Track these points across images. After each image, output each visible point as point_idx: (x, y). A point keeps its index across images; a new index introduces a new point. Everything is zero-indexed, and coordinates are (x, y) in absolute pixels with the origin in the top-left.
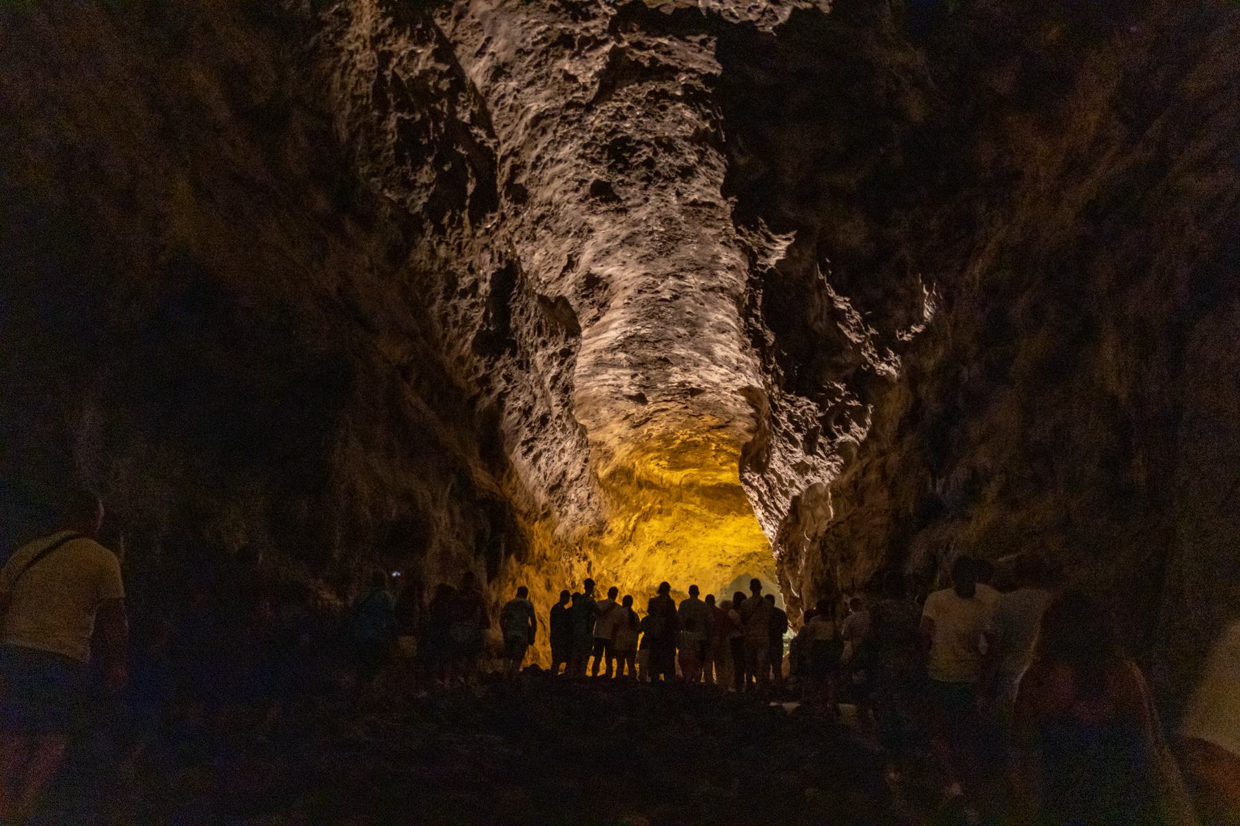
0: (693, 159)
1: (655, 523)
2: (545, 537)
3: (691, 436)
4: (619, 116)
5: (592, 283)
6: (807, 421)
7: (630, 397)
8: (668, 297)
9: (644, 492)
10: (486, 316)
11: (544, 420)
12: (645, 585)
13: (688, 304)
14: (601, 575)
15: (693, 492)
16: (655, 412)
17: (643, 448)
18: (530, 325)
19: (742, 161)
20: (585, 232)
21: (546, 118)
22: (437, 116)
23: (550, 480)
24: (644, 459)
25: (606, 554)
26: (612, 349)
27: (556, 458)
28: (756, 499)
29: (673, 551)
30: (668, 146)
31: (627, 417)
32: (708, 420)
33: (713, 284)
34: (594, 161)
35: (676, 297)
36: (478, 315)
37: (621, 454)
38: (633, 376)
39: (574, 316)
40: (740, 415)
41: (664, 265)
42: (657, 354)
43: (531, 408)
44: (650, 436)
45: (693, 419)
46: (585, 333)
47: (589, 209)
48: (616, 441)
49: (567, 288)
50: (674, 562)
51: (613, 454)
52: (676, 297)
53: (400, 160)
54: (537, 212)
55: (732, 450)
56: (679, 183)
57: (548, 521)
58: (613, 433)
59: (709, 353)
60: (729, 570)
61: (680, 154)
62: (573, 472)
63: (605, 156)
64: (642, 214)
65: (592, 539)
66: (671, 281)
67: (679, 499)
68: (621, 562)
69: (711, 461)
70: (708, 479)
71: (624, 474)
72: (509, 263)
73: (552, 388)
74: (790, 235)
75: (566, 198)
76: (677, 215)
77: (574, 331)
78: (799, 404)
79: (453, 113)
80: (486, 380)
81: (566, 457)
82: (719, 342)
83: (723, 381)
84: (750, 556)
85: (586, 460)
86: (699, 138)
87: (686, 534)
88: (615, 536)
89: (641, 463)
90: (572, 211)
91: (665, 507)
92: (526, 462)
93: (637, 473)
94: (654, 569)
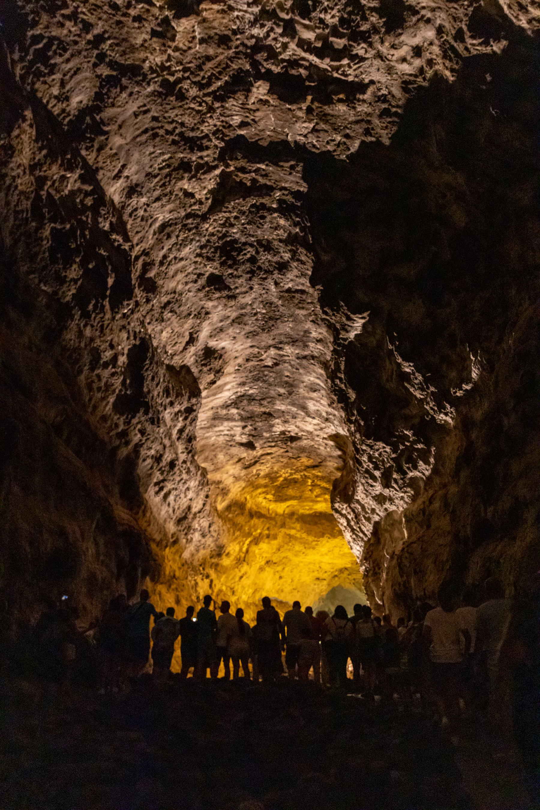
0: (287, 256)
1: (264, 546)
2: (174, 560)
3: (291, 474)
4: (228, 224)
5: (209, 354)
6: (383, 461)
7: (242, 444)
8: (270, 364)
9: (255, 521)
10: (123, 383)
11: (172, 465)
13: (286, 370)
14: (220, 591)
15: (294, 520)
16: (262, 455)
17: (253, 485)
18: (160, 389)
19: (325, 258)
20: (202, 314)
21: (170, 226)
22: (83, 225)
23: (178, 514)
24: (254, 494)
25: (224, 573)
26: (226, 406)
27: (182, 495)
28: (345, 524)
29: (279, 568)
30: (267, 246)
31: (240, 460)
32: (305, 461)
33: (306, 353)
34: (209, 259)
35: (276, 364)
36: (117, 382)
37: (236, 490)
38: (244, 427)
39: (195, 381)
40: (331, 456)
41: (266, 339)
42: (263, 409)
43: (161, 456)
44: (258, 475)
45: (293, 460)
46: (204, 394)
47: (205, 296)
48: (231, 480)
49: (189, 358)
50: (281, 578)
51: (229, 490)
52: (276, 364)
53: (53, 260)
54: (164, 299)
55: (324, 485)
56: (276, 275)
57: (176, 547)
58: (228, 474)
59: (304, 408)
60: (325, 583)
61: (276, 253)
62: (196, 507)
63: (218, 255)
64: (248, 299)
65: (213, 560)
66: (273, 352)
67: (283, 525)
68: (237, 579)
69: (308, 494)
70: (306, 508)
71: (237, 506)
72: (142, 340)
73: (178, 439)
74: (365, 315)
75: (187, 287)
76: (276, 300)
77: (196, 393)
78: (376, 447)
79: (96, 222)
80: (124, 434)
81: (190, 494)
82: (312, 399)
83: (316, 430)
84: (341, 571)
85: (207, 496)
86: (291, 240)
87: (290, 555)
88: (232, 558)
89: (251, 497)
90: (192, 298)
91: (272, 532)
92: (158, 499)
93: (249, 505)
94: (264, 584)
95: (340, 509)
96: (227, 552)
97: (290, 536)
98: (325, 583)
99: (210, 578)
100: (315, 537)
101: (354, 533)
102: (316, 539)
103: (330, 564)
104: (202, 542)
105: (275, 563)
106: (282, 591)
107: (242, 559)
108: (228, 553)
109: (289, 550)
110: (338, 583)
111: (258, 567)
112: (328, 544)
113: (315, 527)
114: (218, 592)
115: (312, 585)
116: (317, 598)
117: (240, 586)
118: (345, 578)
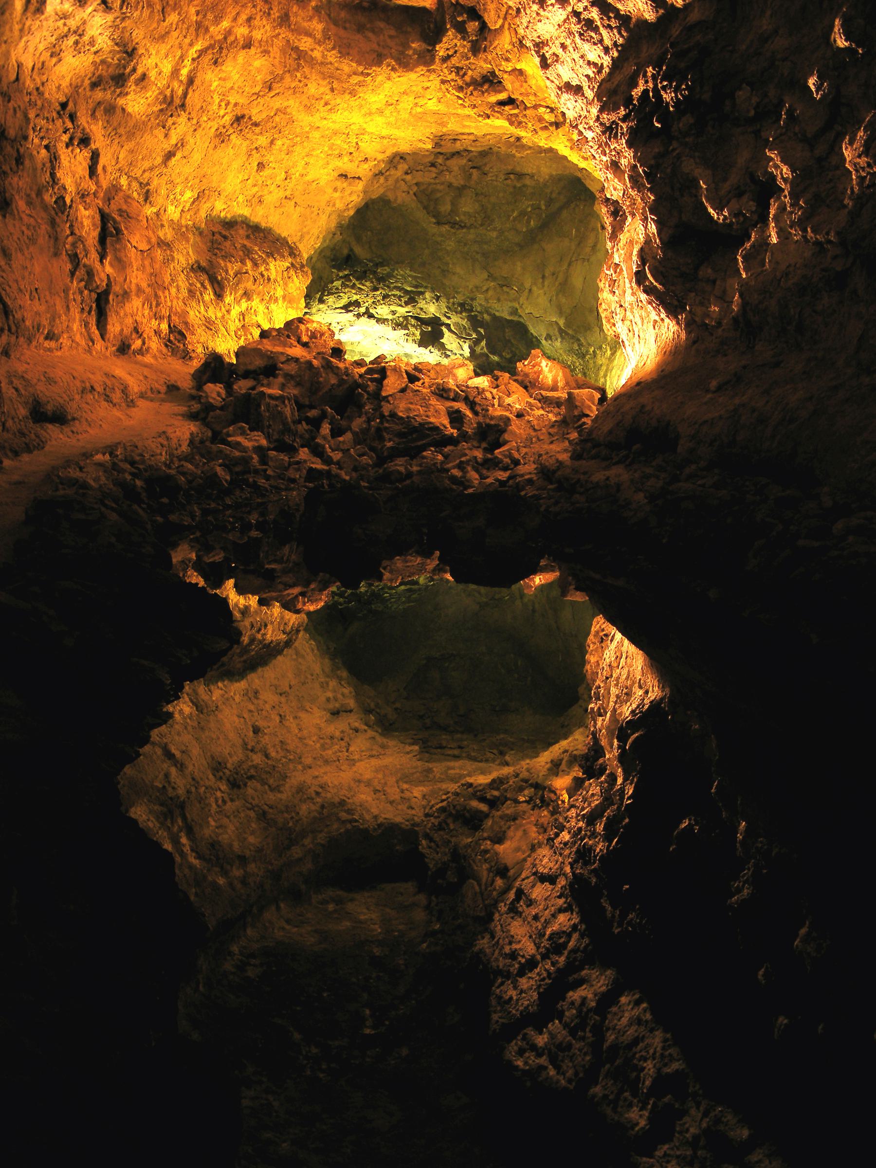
12: (203, 214)
14: (115, 188)
29: (263, 141)
50: (261, 166)
65: (99, 95)
68: (159, 160)
84: (397, 159)
87: (293, 104)
88: (151, 94)
94: (223, 180)
96: (140, 71)
97: (301, 55)
98: (360, 186)
99: (93, 146)
100: (359, 63)
102: (361, 69)
105: (256, 125)
107: (177, 101)
108: (144, 77)
110: (382, 191)
111: (213, 130)
112: (388, 84)
113: (358, 36)
114: (108, 191)
115: (330, 191)
116: (333, 225)
117: (165, 178)
118: (397, 181)
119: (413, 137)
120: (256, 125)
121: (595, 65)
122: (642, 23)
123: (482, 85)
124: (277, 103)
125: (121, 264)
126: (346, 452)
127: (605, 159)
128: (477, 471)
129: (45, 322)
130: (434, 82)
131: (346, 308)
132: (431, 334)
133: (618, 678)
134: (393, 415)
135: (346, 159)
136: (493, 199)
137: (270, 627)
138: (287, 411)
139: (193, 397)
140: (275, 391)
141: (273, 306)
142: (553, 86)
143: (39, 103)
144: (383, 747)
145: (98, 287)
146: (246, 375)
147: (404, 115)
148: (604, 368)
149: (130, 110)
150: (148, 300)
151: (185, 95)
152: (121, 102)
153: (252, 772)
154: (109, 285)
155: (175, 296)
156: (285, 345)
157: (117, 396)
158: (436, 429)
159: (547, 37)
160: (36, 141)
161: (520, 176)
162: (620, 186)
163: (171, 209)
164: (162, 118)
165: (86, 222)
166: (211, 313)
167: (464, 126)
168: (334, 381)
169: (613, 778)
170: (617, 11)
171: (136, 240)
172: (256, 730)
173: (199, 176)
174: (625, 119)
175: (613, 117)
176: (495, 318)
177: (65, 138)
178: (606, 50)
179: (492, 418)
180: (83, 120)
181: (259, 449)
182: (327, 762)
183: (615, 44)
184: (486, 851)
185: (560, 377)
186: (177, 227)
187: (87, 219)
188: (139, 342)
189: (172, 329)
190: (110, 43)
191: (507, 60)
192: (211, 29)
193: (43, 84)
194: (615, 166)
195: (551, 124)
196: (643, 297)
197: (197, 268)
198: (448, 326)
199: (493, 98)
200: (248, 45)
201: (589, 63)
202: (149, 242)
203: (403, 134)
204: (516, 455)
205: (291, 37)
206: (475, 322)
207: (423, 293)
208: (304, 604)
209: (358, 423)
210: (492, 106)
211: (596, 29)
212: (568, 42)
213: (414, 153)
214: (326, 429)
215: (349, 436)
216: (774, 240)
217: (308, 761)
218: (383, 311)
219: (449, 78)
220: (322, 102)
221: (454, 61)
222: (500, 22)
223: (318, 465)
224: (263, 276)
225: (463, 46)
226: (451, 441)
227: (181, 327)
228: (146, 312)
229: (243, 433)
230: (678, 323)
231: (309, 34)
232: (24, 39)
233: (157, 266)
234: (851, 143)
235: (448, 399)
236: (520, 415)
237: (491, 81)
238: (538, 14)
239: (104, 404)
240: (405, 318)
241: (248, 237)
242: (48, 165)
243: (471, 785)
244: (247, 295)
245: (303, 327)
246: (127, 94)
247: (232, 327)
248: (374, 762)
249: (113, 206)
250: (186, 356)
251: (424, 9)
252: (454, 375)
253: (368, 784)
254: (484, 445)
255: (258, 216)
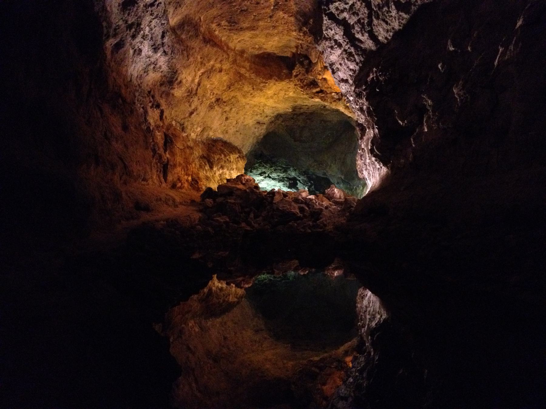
14: (171, 125)
28: (339, 37)
29: (227, 109)
50: (227, 119)
65: (163, 89)
68: (187, 115)
84: (279, 116)
87: (238, 94)
88: (183, 89)
93: (202, 29)
95: (336, 13)
96: (179, 79)
98: (265, 127)
100: (263, 78)
101: (353, 45)
102: (264, 81)
103: (273, 107)
104: (152, 60)
105: (225, 102)
106: (227, 132)
107: (194, 92)
109: (239, 89)
112: (274, 87)
115: (253, 128)
118: (279, 125)
119: (284, 107)
120: (225, 102)
121: (353, 70)
122: (371, 51)
123: (310, 86)
124: (232, 94)
125: (173, 154)
126: (259, 224)
127: (357, 107)
128: (309, 229)
129: (142, 174)
130: (292, 85)
131: (261, 174)
132: (293, 184)
133: (369, 311)
134: (278, 209)
135: (259, 116)
136: (316, 131)
137: (231, 296)
138: (237, 208)
139: (200, 204)
140: (233, 201)
141: (232, 172)
142: (337, 81)
143: (140, 90)
144: (276, 345)
145: (163, 162)
146: (221, 195)
147: (281, 98)
148: (360, 194)
149: (175, 95)
150: (183, 168)
151: (197, 89)
152: (172, 91)
153: (223, 356)
154: (168, 161)
155: (194, 166)
156: (236, 184)
157: (171, 202)
158: (294, 214)
159: (334, 61)
160: (139, 105)
161: (325, 122)
162: (363, 117)
163: (192, 134)
164: (188, 98)
165: (159, 137)
166: (208, 174)
167: (304, 102)
168: (255, 197)
169: (369, 353)
170: (361, 48)
171: (179, 145)
172: (225, 338)
173: (205, 123)
174: (364, 90)
175: (360, 90)
176: (317, 177)
177: (150, 104)
178: (357, 64)
179: (316, 209)
180: (157, 98)
181: (226, 223)
182: (253, 352)
183: (361, 61)
184: (319, 389)
185: (342, 195)
186: (195, 141)
187: (159, 136)
188: (180, 184)
189: (193, 179)
190: (167, 68)
191: (320, 74)
192: (207, 64)
193: (141, 83)
194: (361, 110)
195: (337, 99)
196: (373, 159)
197: (202, 157)
198: (299, 181)
199: (315, 91)
200: (221, 71)
201: (351, 70)
202: (184, 146)
203: (280, 106)
204: (325, 223)
205: (237, 68)
206: (310, 179)
207: (289, 168)
208: (244, 284)
209: (264, 213)
210: (314, 94)
211: (353, 56)
212: (342, 62)
213: (285, 114)
214: (252, 215)
215: (261, 218)
216: (426, 130)
217: (245, 351)
218: (274, 175)
219: (298, 83)
220: (250, 94)
221: (299, 76)
222: (316, 60)
223: (248, 228)
224: (228, 160)
225: (303, 70)
226: (299, 218)
227: (197, 179)
228: (183, 173)
229: (220, 216)
230: (388, 168)
231: (244, 67)
232: (133, 65)
233: (187, 155)
234: (457, 87)
235: (298, 203)
236: (326, 208)
237: (314, 84)
238: (330, 52)
239: (165, 205)
240: (283, 178)
241: (222, 146)
242: (143, 115)
243: (312, 361)
244: (222, 167)
245: (243, 178)
246: (174, 88)
247: (216, 180)
248: (272, 351)
249: (170, 132)
250: (198, 190)
251: (287, 57)
252: (301, 195)
253: (270, 360)
254: (313, 220)
255: (226, 138)
